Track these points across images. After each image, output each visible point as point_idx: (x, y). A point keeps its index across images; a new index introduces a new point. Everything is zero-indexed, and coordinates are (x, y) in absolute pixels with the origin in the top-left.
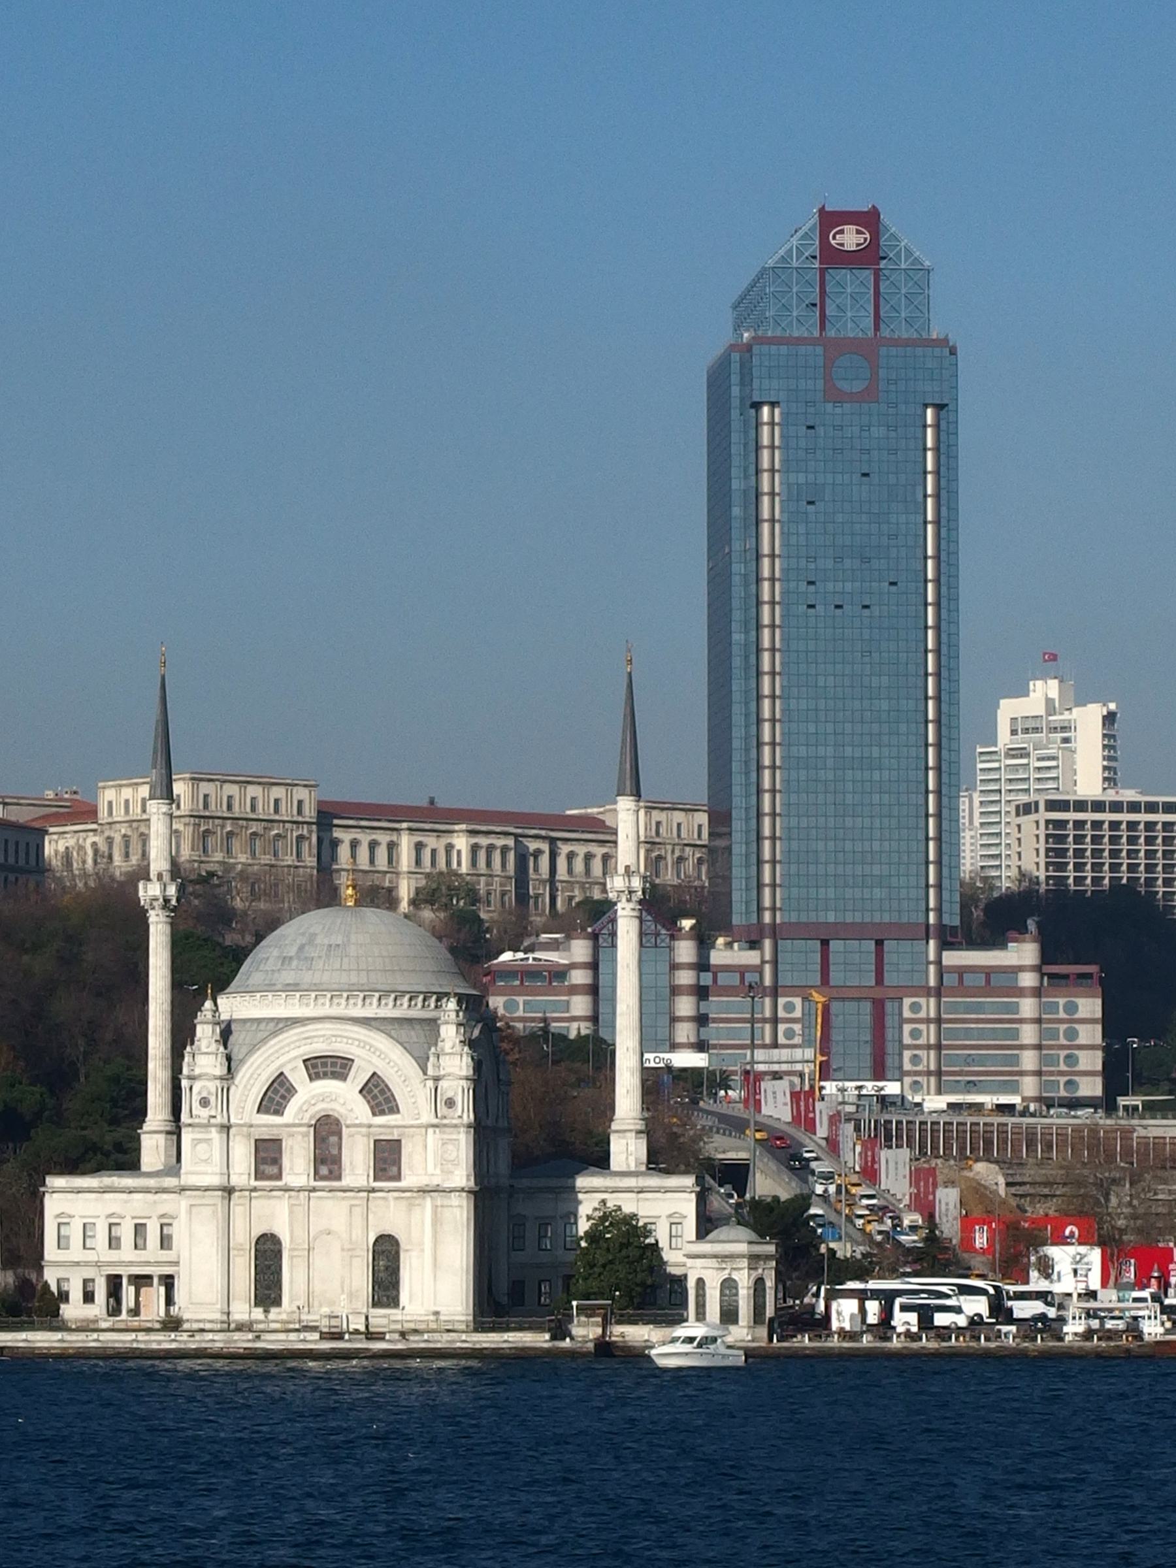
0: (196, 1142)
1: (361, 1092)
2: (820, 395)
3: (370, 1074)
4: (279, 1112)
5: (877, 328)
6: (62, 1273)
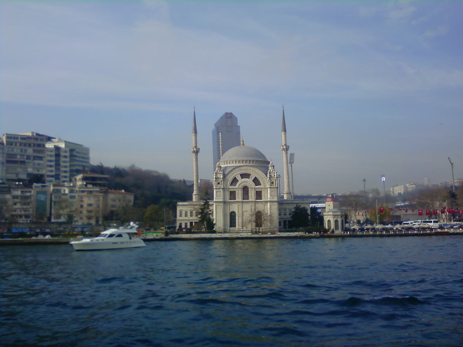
0: (217, 192)
3: (254, 177)
6: (181, 222)
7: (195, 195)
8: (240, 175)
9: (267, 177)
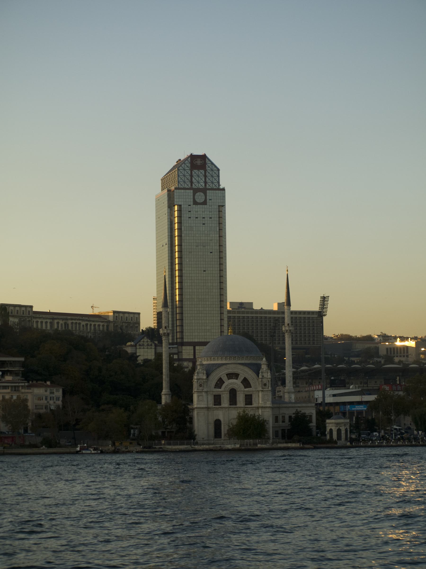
0: (198, 396)
1: (241, 382)
2: (192, 203)
4: (220, 388)
5: (205, 185)
7: (165, 394)
8: (227, 375)
9: (258, 376)
